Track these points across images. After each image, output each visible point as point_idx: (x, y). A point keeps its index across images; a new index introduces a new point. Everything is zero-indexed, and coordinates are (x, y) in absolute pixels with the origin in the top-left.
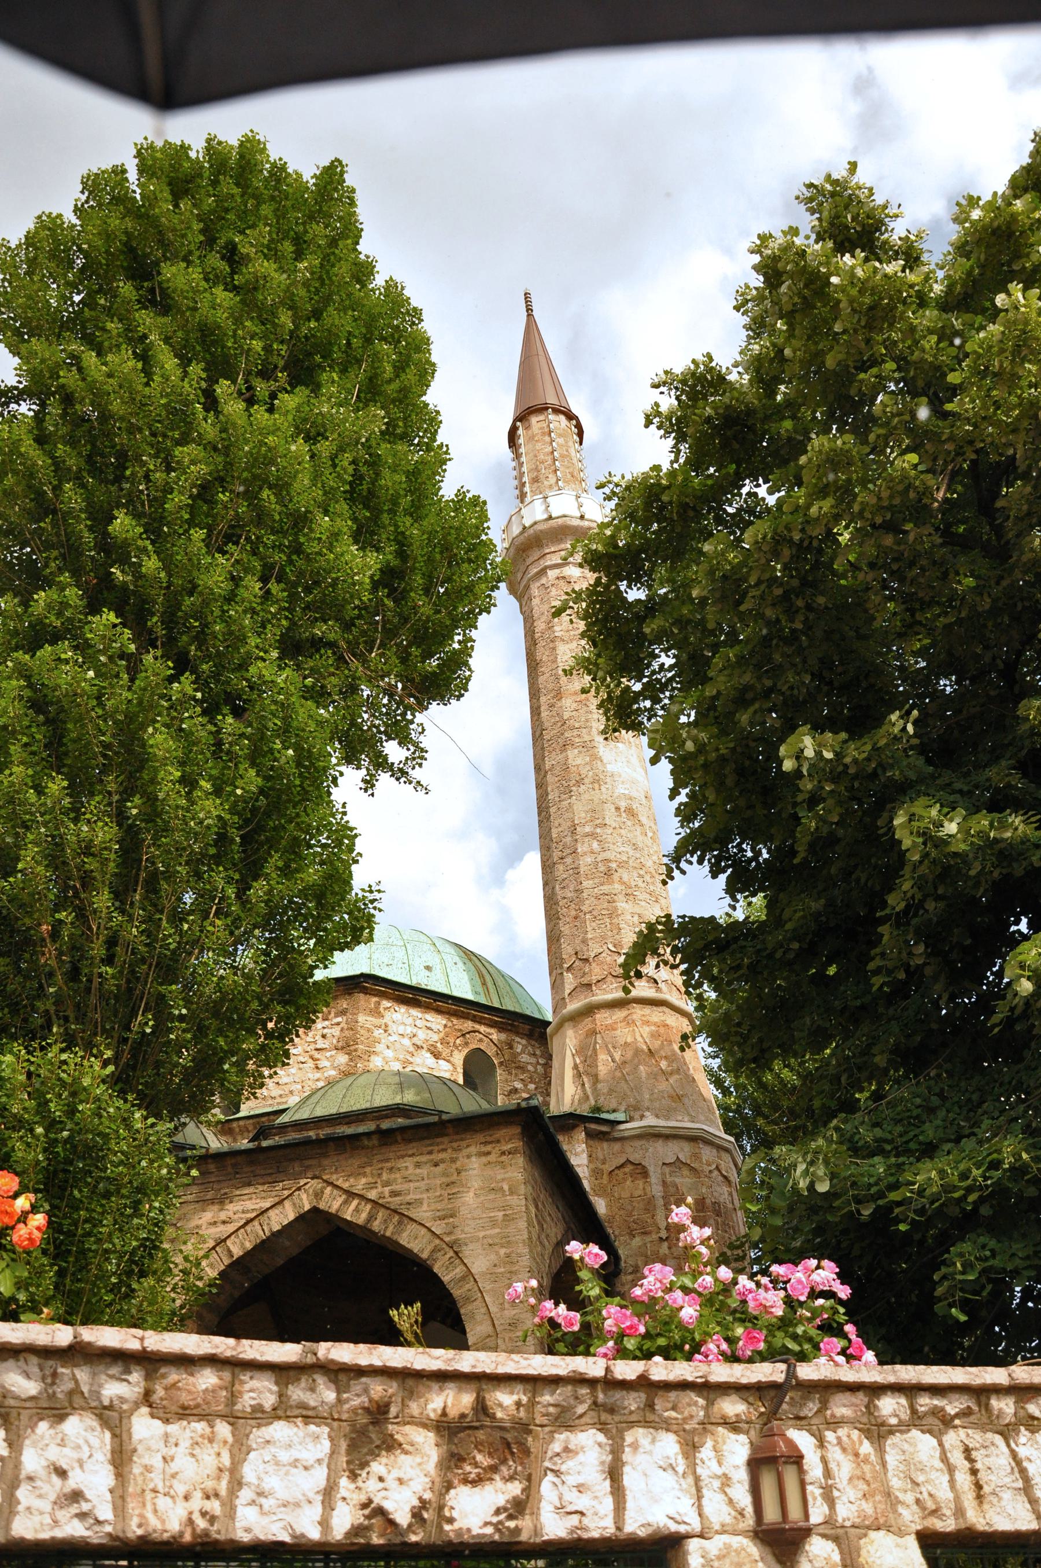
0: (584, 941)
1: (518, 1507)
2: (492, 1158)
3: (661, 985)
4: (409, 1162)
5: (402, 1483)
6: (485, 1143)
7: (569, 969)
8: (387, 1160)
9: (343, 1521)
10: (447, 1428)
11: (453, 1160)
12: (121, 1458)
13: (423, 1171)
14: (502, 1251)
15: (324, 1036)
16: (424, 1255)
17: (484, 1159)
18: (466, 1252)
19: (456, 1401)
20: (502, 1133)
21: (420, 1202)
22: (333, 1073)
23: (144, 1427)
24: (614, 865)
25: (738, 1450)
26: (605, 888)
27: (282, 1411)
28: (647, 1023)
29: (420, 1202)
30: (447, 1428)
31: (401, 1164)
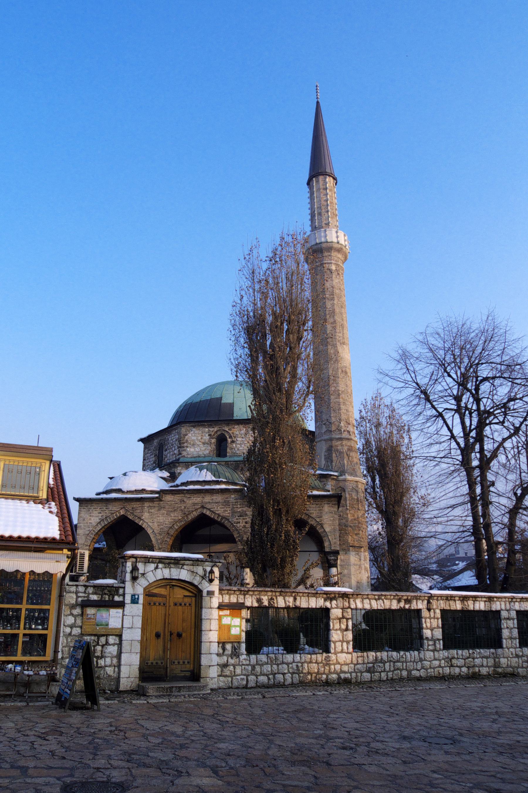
0: (330, 417)
1: (410, 606)
2: (330, 505)
3: (351, 433)
5: (402, 604)
7: (324, 424)
9: (398, 608)
10: (405, 600)
11: (321, 504)
12: (384, 603)
13: (314, 506)
16: (315, 525)
18: (324, 526)
19: (405, 598)
20: (333, 499)
23: (385, 600)
24: (340, 392)
25: (426, 602)
26: (338, 400)
27: (394, 599)
28: (346, 445)
30: (405, 600)
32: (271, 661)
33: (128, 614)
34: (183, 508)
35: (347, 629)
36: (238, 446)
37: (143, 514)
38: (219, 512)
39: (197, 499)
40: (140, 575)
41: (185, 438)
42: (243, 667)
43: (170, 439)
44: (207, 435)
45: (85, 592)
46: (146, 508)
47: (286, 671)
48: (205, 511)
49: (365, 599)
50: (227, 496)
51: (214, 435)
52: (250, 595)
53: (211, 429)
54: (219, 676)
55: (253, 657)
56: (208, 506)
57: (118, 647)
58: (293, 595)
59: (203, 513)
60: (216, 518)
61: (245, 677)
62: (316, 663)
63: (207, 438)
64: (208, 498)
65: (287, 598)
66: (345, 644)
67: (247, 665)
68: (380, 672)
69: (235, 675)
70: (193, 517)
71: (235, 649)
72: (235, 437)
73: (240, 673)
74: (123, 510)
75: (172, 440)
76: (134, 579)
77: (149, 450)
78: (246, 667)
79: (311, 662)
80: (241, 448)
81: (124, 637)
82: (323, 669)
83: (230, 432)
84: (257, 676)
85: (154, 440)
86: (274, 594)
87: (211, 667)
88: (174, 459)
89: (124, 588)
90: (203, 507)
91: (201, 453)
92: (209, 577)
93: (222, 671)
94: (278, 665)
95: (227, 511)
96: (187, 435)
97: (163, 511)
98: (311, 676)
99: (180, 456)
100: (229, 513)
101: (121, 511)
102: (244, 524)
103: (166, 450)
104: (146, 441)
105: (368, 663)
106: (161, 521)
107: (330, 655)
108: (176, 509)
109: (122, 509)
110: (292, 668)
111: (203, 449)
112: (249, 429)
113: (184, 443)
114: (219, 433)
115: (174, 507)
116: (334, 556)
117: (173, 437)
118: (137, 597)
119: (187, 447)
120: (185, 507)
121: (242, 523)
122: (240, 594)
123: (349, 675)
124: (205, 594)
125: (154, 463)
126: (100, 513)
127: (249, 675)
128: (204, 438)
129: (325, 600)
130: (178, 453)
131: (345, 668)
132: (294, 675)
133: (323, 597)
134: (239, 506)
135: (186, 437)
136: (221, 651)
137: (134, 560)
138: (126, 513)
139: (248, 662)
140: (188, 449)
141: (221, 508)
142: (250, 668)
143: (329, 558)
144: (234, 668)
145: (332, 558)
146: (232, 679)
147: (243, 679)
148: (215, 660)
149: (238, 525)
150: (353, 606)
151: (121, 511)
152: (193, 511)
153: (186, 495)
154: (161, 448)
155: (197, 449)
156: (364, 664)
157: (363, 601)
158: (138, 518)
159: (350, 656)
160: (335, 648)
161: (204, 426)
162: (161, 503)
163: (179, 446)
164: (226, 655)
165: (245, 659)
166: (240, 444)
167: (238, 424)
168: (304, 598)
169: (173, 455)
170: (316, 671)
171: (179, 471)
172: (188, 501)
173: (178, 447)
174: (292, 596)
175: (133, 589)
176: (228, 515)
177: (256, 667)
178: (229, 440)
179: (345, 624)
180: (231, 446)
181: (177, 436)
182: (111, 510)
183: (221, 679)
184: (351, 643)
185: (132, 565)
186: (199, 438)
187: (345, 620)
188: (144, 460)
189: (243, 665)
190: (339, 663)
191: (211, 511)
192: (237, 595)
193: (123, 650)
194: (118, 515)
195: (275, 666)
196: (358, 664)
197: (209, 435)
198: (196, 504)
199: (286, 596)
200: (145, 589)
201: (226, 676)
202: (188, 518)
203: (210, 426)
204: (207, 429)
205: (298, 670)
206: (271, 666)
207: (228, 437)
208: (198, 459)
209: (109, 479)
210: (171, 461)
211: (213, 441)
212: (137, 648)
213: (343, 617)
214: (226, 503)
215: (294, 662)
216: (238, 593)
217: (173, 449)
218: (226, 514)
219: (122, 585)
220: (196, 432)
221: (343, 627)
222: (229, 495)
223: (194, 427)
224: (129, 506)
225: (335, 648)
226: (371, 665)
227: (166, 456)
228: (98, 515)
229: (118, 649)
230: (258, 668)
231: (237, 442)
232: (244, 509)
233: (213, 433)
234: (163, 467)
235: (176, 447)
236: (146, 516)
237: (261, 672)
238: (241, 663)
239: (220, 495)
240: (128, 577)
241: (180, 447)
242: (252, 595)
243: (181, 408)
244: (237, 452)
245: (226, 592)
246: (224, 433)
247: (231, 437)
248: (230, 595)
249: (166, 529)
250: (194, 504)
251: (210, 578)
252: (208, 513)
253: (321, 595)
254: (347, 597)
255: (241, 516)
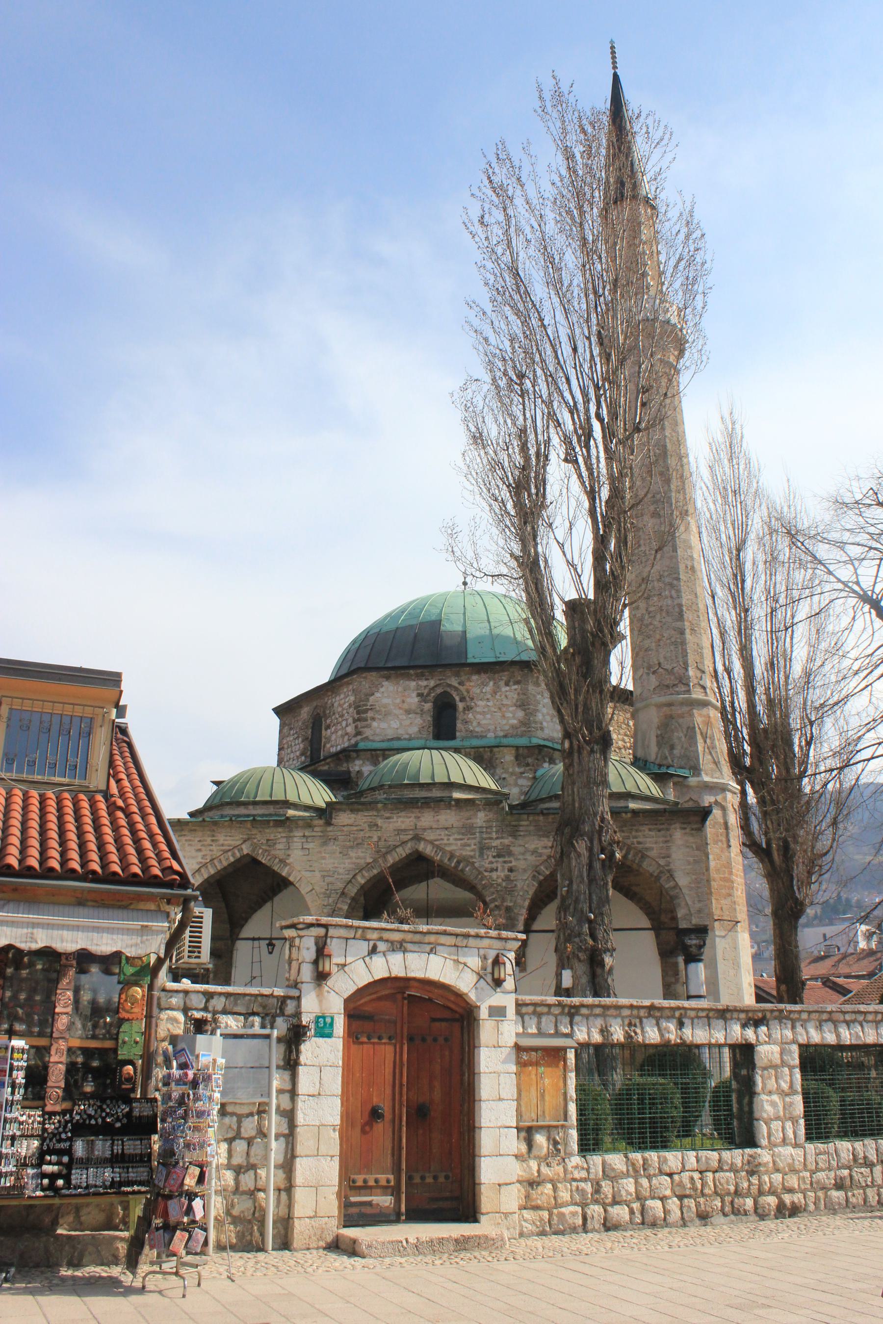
2: (688, 830)
3: (708, 690)
4: (645, 828)
6: (684, 823)
8: (635, 825)
13: (653, 833)
14: (694, 877)
15: (506, 696)
17: (683, 831)
21: (652, 849)
22: (515, 722)
29: (652, 849)
31: (642, 828)
32: (636, 1171)
33: (308, 1062)
34: (375, 839)
35: (792, 1091)
36: (479, 716)
37: (290, 852)
38: (453, 847)
39: (404, 821)
40: (334, 969)
41: (368, 700)
42: (574, 1184)
43: (336, 705)
44: (414, 695)
45: (205, 1009)
46: (295, 839)
47: (668, 1192)
48: (421, 847)
49: (826, 1021)
50: (468, 814)
51: (428, 694)
52: (582, 1015)
53: (424, 683)
54: (523, 1208)
55: (596, 1160)
56: (430, 836)
57: (287, 1143)
58: (677, 1014)
59: (417, 851)
60: (446, 861)
61: (579, 1209)
62: (730, 1170)
63: (413, 700)
64: (427, 819)
65: (664, 1024)
66: (789, 1124)
67: (584, 1180)
68: (864, 1188)
69: (557, 1206)
70: (397, 859)
71: (556, 1143)
72: (472, 699)
73: (569, 1199)
74: (248, 843)
75: (340, 705)
76: (321, 977)
77: (291, 729)
78: (582, 1185)
79: (720, 1169)
80: (483, 722)
81: (300, 1118)
82: (745, 1185)
83: (461, 687)
84: (604, 1206)
85: (301, 707)
86: (635, 1012)
87: (503, 1188)
88: (346, 745)
89: (299, 998)
90: (417, 838)
91: (401, 731)
92: (493, 974)
93: (527, 1197)
94: (649, 1178)
95: (469, 845)
96: (373, 694)
97: (332, 847)
98: (723, 1201)
99: (359, 737)
100: (473, 850)
101: (244, 846)
102: (506, 872)
103: (328, 727)
104: (284, 711)
105: (839, 1168)
106: (330, 866)
107: (759, 1150)
108: (360, 841)
109: (245, 841)
110: (681, 1184)
111: (408, 722)
112: (502, 683)
113: (366, 711)
114: (439, 691)
115: (356, 839)
116: (698, 938)
117: (344, 700)
118: (328, 1020)
119: (373, 719)
120: (380, 838)
121: (503, 870)
122: (562, 1013)
123: (801, 1196)
124: (484, 1013)
125: (302, 754)
126: (200, 850)
127: (587, 1205)
128: (408, 700)
129: (744, 1026)
130: (354, 732)
131: (793, 1181)
132: (686, 1200)
133: (738, 1019)
134: (494, 835)
135: (371, 698)
136: (524, 1148)
137: (321, 931)
138: (253, 850)
139: (584, 1174)
140: (375, 724)
141: (456, 839)
142: (588, 1187)
143: (689, 942)
144: (555, 1189)
145: (694, 942)
146: (551, 1214)
147: (574, 1214)
148: (516, 1170)
149: (494, 875)
150: (802, 1040)
151: (244, 846)
152: (397, 847)
153: (382, 812)
154: (317, 724)
155: (395, 724)
156: (829, 1169)
157: (821, 1025)
158: (281, 861)
159: (800, 1152)
160: (769, 1135)
161: (409, 677)
162: (330, 828)
163: (356, 716)
164: (535, 1158)
165: (576, 1167)
166: (483, 713)
167: (478, 672)
168: (700, 1021)
169: (342, 736)
170: (732, 1188)
171: (357, 768)
172: (385, 826)
173: (355, 721)
174: (673, 1017)
175: (320, 1002)
176: (472, 853)
177: (603, 1184)
178: (461, 706)
179: (788, 1078)
180: (465, 717)
181: (352, 698)
182: (223, 845)
183: (527, 1214)
184: (802, 1122)
185: (316, 944)
186: (398, 701)
187: (786, 1070)
188: (281, 749)
189: (574, 1180)
190: (778, 1170)
191: (434, 846)
192: (556, 1016)
193: (299, 1149)
194: (238, 855)
195: (644, 1182)
196: (817, 1170)
197: (419, 695)
198: (405, 830)
199: (661, 1017)
200: (347, 1001)
201: (536, 1208)
202: (386, 860)
203: (419, 677)
204: (413, 684)
205: (694, 1188)
206: (636, 1182)
207: (457, 698)
208: (396, 744)
209: (215, 788)
210: (339, 748)
211: (428, 706)
212: (332, 1142)
213: (784, 1063)
214: (468, 830)
215: (683, 1170)
216: (557, 1012)
217: (344, 724)
218: (467, 852)
219: (294, 993)
220: (391, 688)
221: (785, 1086)
222: (471, 813)
223: (388, 678)
224: (260, 838)
225: (769, 1135)
226: (846, 1172)
227: (328, 740)
228: (194, 854)
229: (287, 1146)
230: (607, 1188)
231: (478, 709)
232: (506, 841)
233: (426, 692)
234: (324, 760)
235: (350, 720)
236: (296, 856)
237: (614, 1197)
238: (569, 1176)
239: (453, 813)
240: (307, 972)
241: (359, 720)
242: (587, 1017)
243: (357, 645)
244: (477, 729)
245: (530, 1009)
246: (449, 690)
247: (462, 699)
248: (539, 1016)
249: (340, 885)
250: (399, 831)
251: (496, 976)
252: (427, 850)
253: (735, 1015)
254: (787, 1018)
255: (499, 856)
